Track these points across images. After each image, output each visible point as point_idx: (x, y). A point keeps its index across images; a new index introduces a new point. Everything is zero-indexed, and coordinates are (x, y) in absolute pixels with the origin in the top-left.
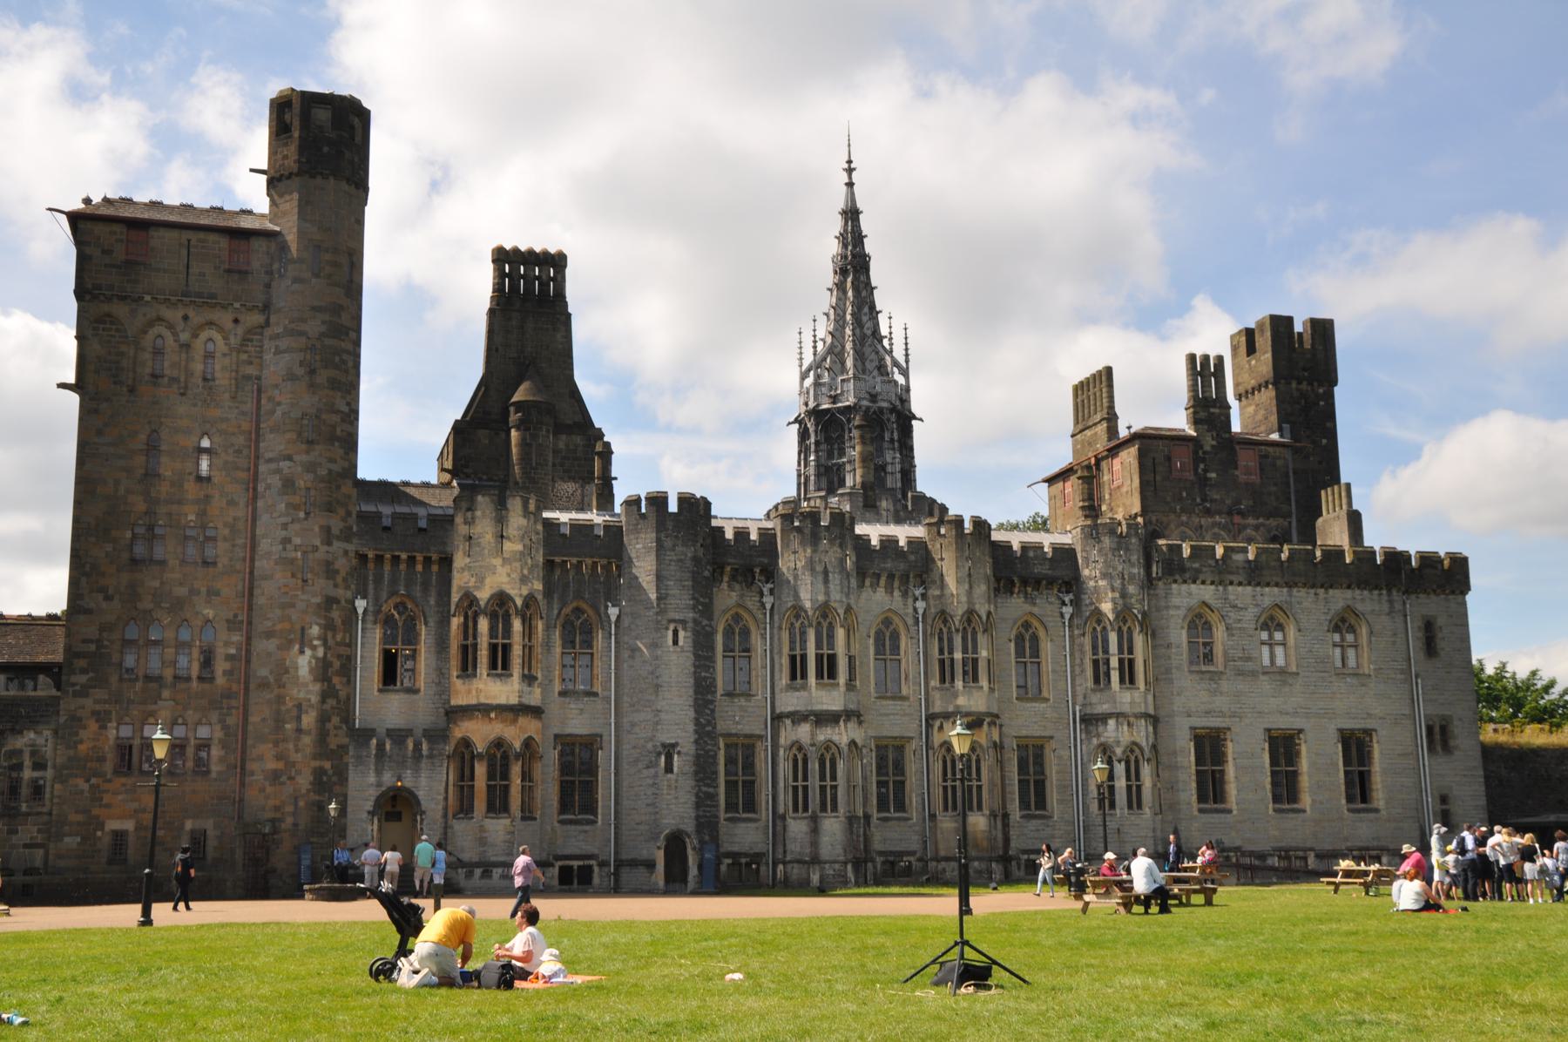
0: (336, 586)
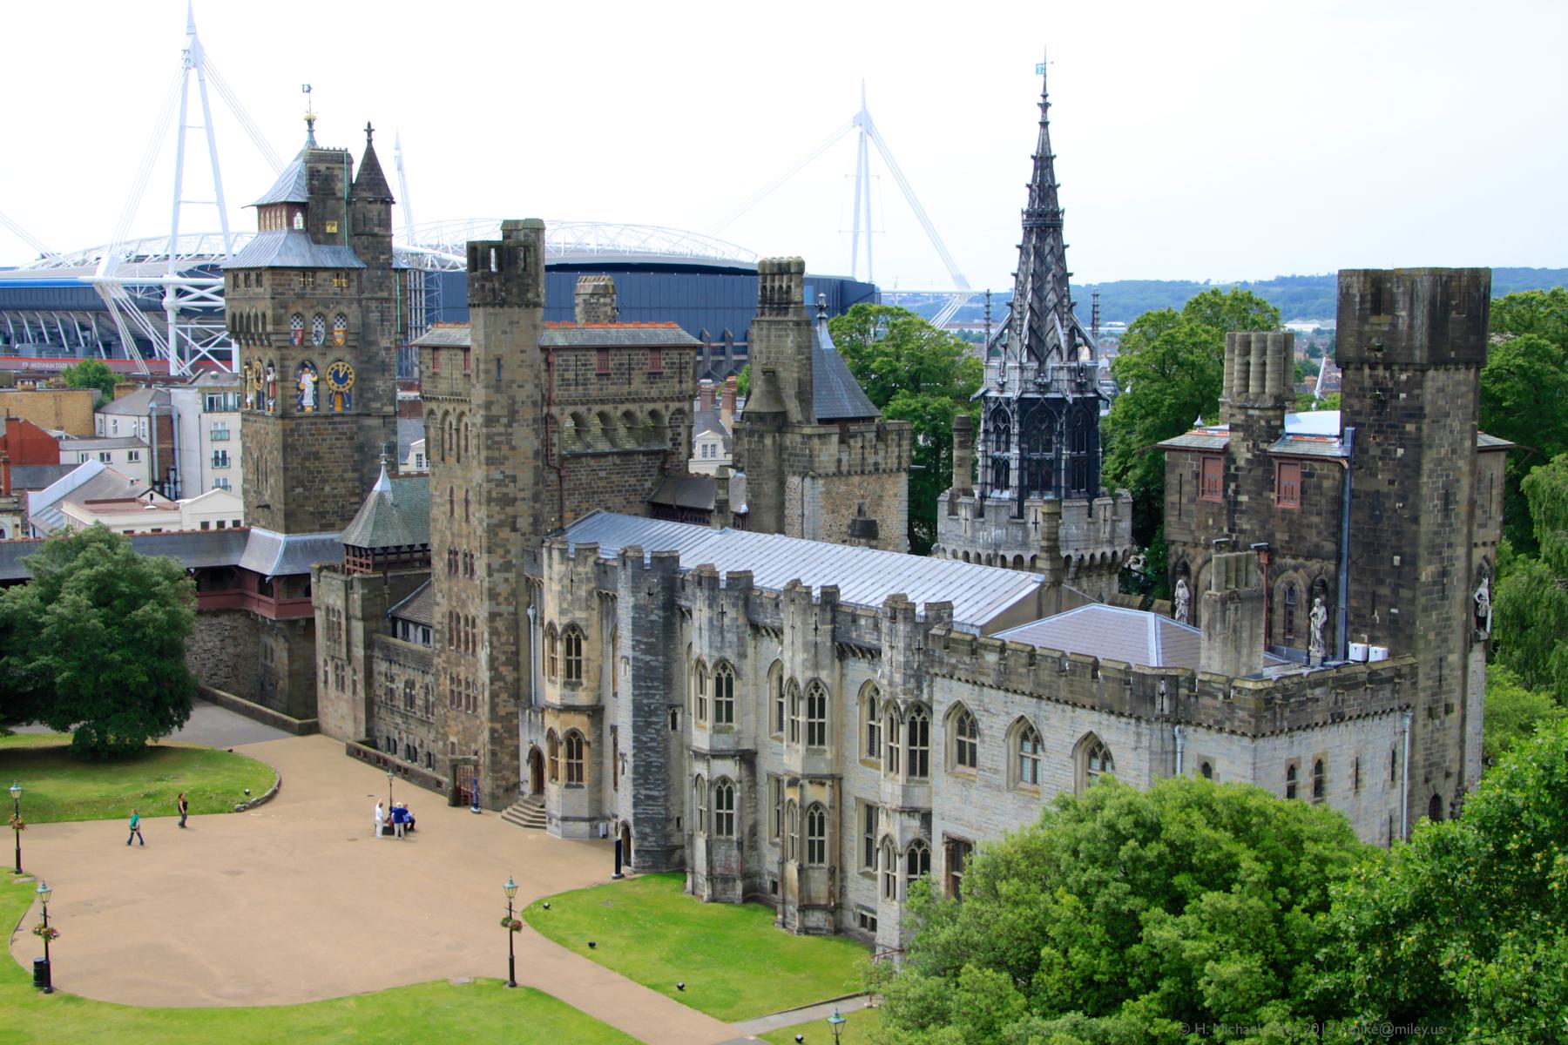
0: (498, 604)
